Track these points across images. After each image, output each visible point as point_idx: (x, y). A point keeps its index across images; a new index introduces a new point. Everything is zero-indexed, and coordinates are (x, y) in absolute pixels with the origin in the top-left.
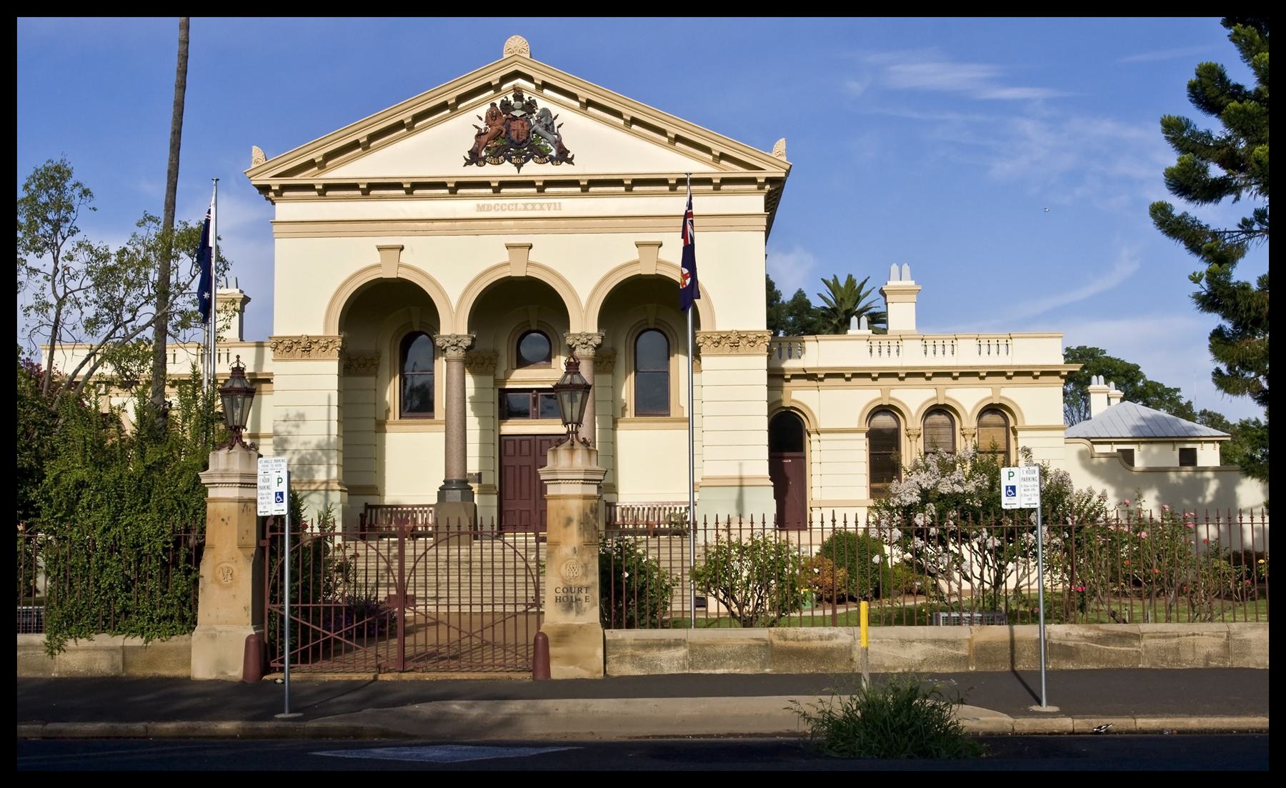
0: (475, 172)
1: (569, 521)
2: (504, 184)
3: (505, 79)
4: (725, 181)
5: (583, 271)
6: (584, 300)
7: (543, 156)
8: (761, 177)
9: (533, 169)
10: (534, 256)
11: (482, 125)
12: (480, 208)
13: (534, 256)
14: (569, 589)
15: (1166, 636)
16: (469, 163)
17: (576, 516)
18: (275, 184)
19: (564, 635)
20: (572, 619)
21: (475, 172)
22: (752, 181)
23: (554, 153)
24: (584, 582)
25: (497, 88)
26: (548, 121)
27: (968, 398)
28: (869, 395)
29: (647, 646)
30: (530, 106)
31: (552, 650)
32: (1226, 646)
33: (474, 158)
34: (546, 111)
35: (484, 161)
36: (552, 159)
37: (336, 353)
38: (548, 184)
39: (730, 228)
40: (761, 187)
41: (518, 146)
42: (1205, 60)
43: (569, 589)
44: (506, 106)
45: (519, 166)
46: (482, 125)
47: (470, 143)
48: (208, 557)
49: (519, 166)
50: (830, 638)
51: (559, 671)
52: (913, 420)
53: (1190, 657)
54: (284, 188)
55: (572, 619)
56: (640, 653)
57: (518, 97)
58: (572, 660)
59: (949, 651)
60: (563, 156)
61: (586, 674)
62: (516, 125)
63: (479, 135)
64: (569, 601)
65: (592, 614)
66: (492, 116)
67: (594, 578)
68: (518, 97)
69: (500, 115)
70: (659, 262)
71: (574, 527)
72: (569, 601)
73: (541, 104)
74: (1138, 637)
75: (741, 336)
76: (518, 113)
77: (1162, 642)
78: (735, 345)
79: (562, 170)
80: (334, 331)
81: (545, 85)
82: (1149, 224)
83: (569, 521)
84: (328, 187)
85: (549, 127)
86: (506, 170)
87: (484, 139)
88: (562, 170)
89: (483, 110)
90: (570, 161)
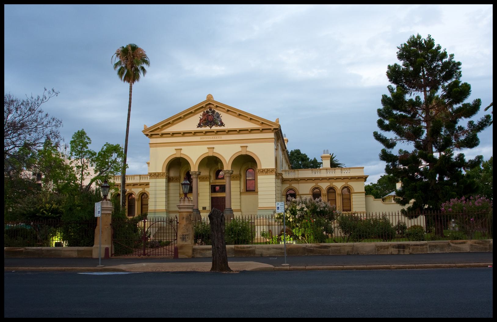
0: (200, 129)
1: (183, 218)
2: (206, 132)
3: (207, 105)
4: (263, 129)
6: (227, 161)
7: (217, 125)
8: (272, 128)
9: (214, 128)
11: (201, 117)
12: (201, 138)
14: (183, 235)
15: (337, 246)
16: (198, 127)
17: (185, 217)
18: (150, 134)
19: (182, 247)
20: (184, 243)
21: (200, 129)
22: (270, 129)
25: (205, 107)
26: (218, 116)
27: (339, 185)
28: (312, 185)
29: (203, 250)
30: (213, 112)
31: (179, 251)
32: (353, 249)
33: (199, 126)
34: (217, 113)
35: (202, 126)
37: (165, 177)
38: (217, 132)
39: (156, 147)
40: (273, 131)
41: (211, 122)
42: (383, 94)
43: (183, 235)
44: (207, 112)
45: (211, 127)
46: (201, 117)
47: (199, 122)
48: (97, 227)
49: (211, 127)
50: (249, 247)
51: (180, 256)
52: (324, 192)
53: (343, 252)
54: (152, 135)
55: (184, 243)
56: (202, 252)
57: (211, 110)
59: (280, 251)
60: (222, 124)
62: (209, 117)
64: (183, 238)
65: (189, 242)
66: (204, 115)
68: (211, 110)
69: (206, 114)
70: (181, 154)
71: (185, 219)
72: (183, 238)
74: (329, 247)
75: (268, 170)
76: (210, 114)
77: (336, 248)
78: (267, 172)
79: (222, 128)
80: (164, 171)
81: (217, 106)
82: (373, 138)
83: (183, 218)
84: (162, 134)
85: (218, 117)
86: (208, 128)
88: (222, 128)
89: (202, 113)
90: (224, 126)
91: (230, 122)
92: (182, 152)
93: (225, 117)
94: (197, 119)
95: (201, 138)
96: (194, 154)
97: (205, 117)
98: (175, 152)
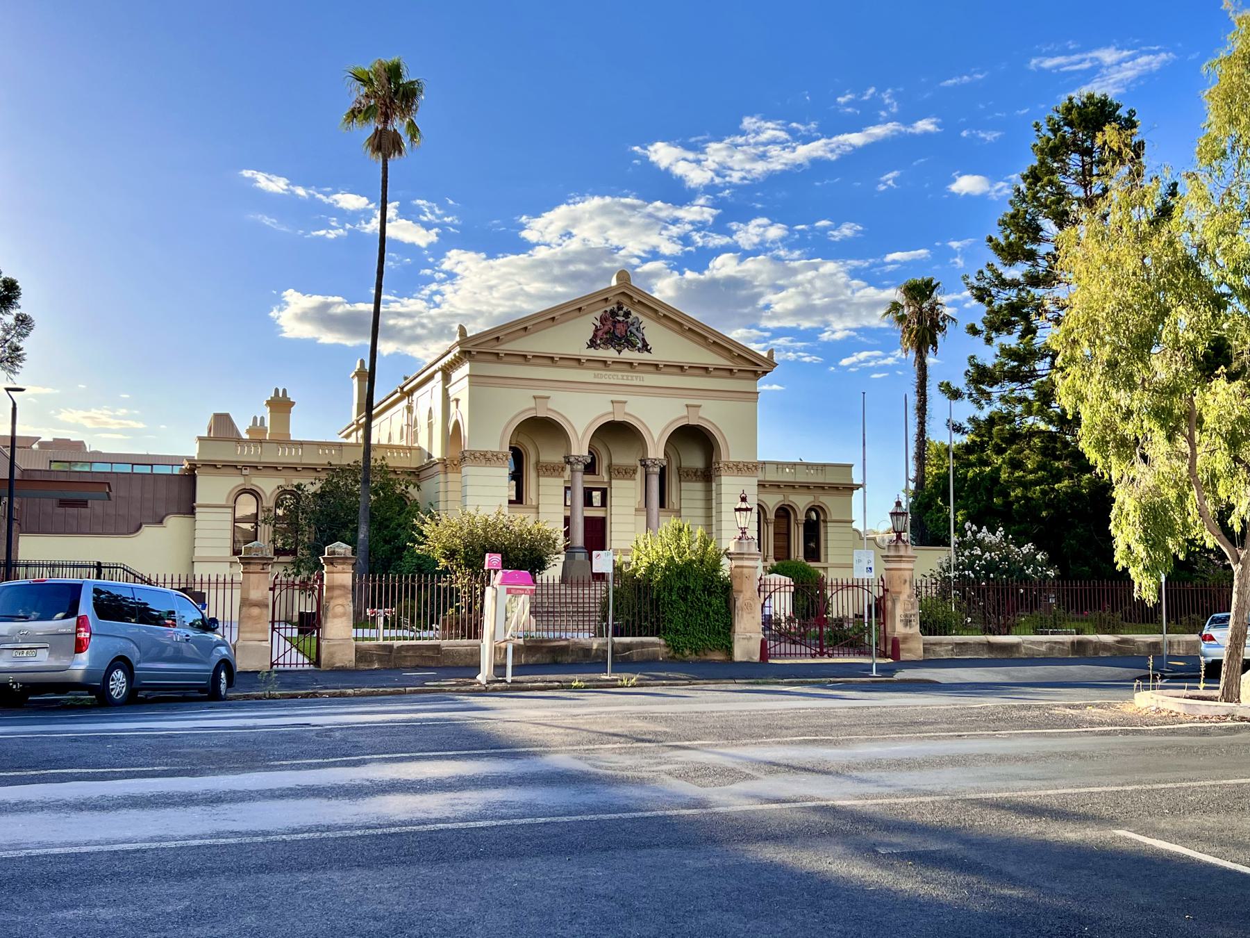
5: (656, 418)
7: (632, 345)
9: (627, 354)
10: (628, 409)
11: (598, 324)
12: (595, 376)
13: (628, 409)
14: (906, 616)
16: (589, 347)
19: (906, 638)
21: (592, 353)
23: (640, 345)
24: (913, 612)
30: (627, 314)
33: (593, 344)
36: (639, 350)
44: (612, 312)
45: (619, 352)
49: (619, 352)
51: (904, 656)
55: (908, 631)
58: (909, 651)
60: (646, 347)
61: (914, 658)
62: (618, 325)
63: (597, 330)
65: (916, 628)
66: (603, 320)
67: (916, 611)
72: (907, 622)
73: (634, 314)
76: (621, 319)
79: (645, 356)
86: (610, 353)
87: (600, 333)
89: (598, 314)
90: (649, 351)
91: (664, 344)
92: (550, 406)
93: (652, 331)
94: (586, 326)
95: (595, 376)
96: (581, 415)
97: (609, 324)
98: (532, 404)
